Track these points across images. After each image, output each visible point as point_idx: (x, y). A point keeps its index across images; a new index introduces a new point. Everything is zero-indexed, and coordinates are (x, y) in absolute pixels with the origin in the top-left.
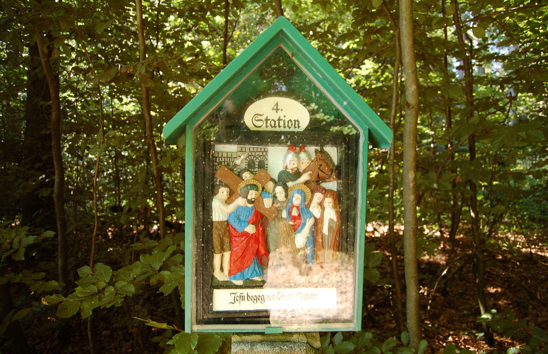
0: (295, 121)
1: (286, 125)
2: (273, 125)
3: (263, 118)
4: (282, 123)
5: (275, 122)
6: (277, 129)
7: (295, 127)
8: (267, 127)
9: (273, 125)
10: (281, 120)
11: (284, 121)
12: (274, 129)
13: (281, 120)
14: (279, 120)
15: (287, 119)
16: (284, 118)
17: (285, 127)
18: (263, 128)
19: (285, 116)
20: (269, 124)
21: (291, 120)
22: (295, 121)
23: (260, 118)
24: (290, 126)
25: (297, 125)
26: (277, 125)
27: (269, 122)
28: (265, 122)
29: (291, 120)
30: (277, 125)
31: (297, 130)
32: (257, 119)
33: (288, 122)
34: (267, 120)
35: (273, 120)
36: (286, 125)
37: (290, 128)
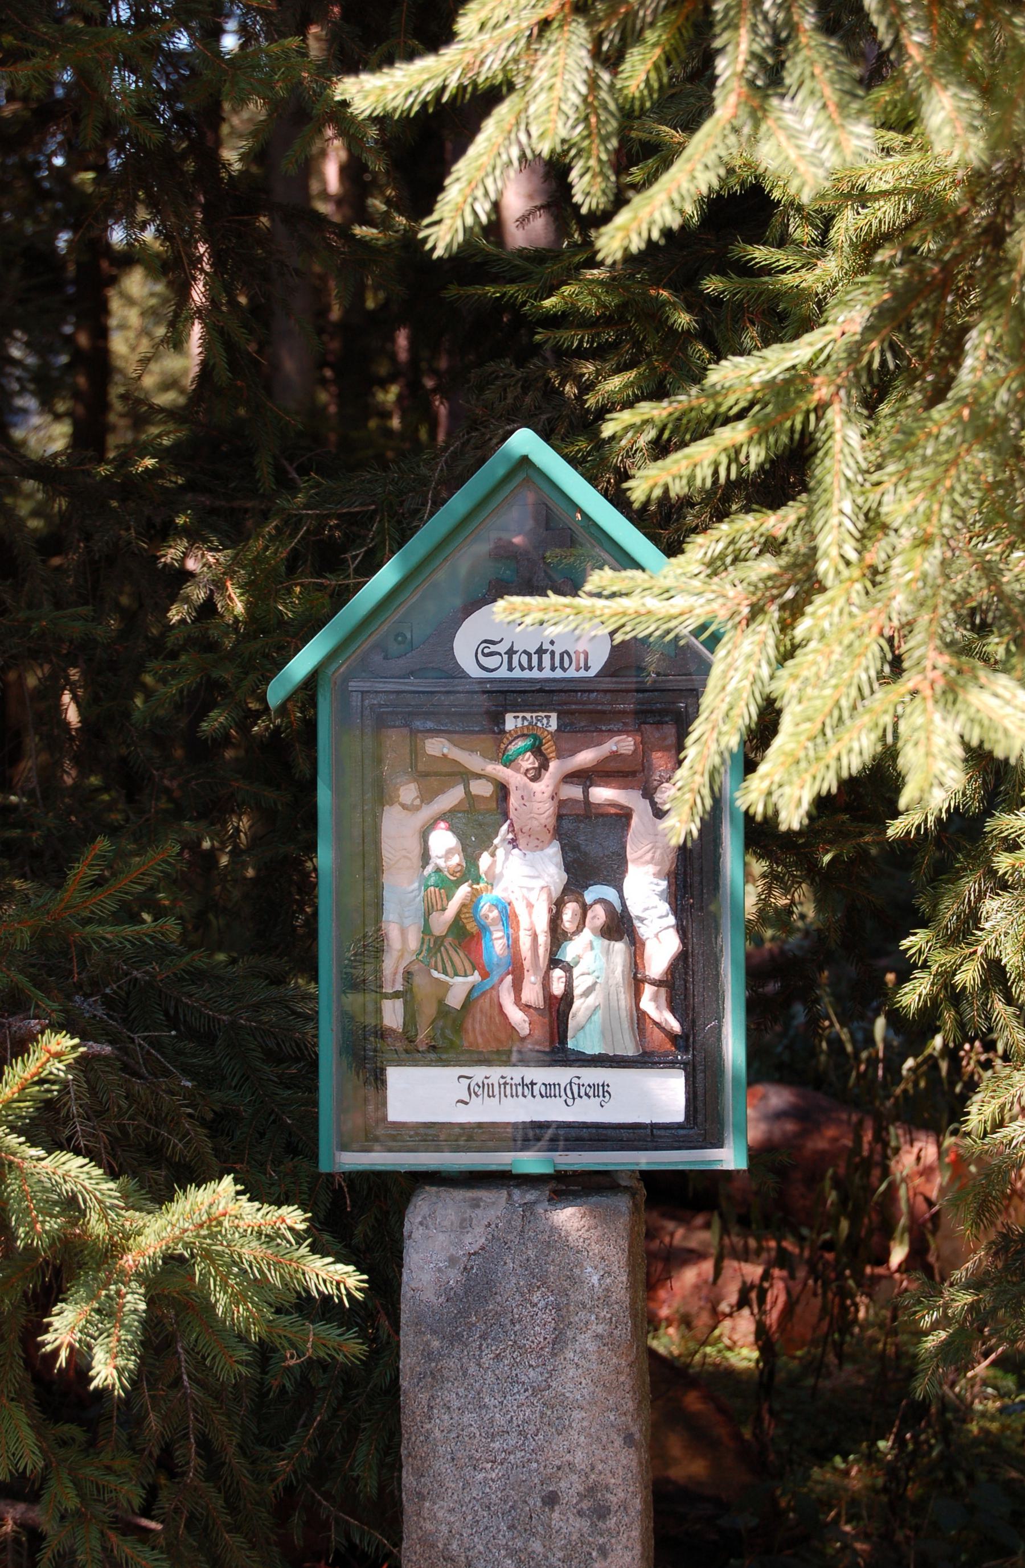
2: (525, 665)
3: (502, 648)
4: (546, 658)
5: (529, 655)
6: (535, 674)
8: (510, 669)
9: (525, 665)
11: (553, 653)
12: (527, 674)
14: (540, 651)
15: (558, 649)
16: (551, 648)
17: (553, 668)
18: (503, 673)
19: (552, 643)
20: (515, 663)
23: (493, 648)
25: (582, 664)
27: (515, 657)
28: (506, 657)
29: (567, 652)
31: (582, 673)
32: (486, 651)
34: (511, 652)
35: (525, 652)
36: (557, 663)
37: (564, 670)
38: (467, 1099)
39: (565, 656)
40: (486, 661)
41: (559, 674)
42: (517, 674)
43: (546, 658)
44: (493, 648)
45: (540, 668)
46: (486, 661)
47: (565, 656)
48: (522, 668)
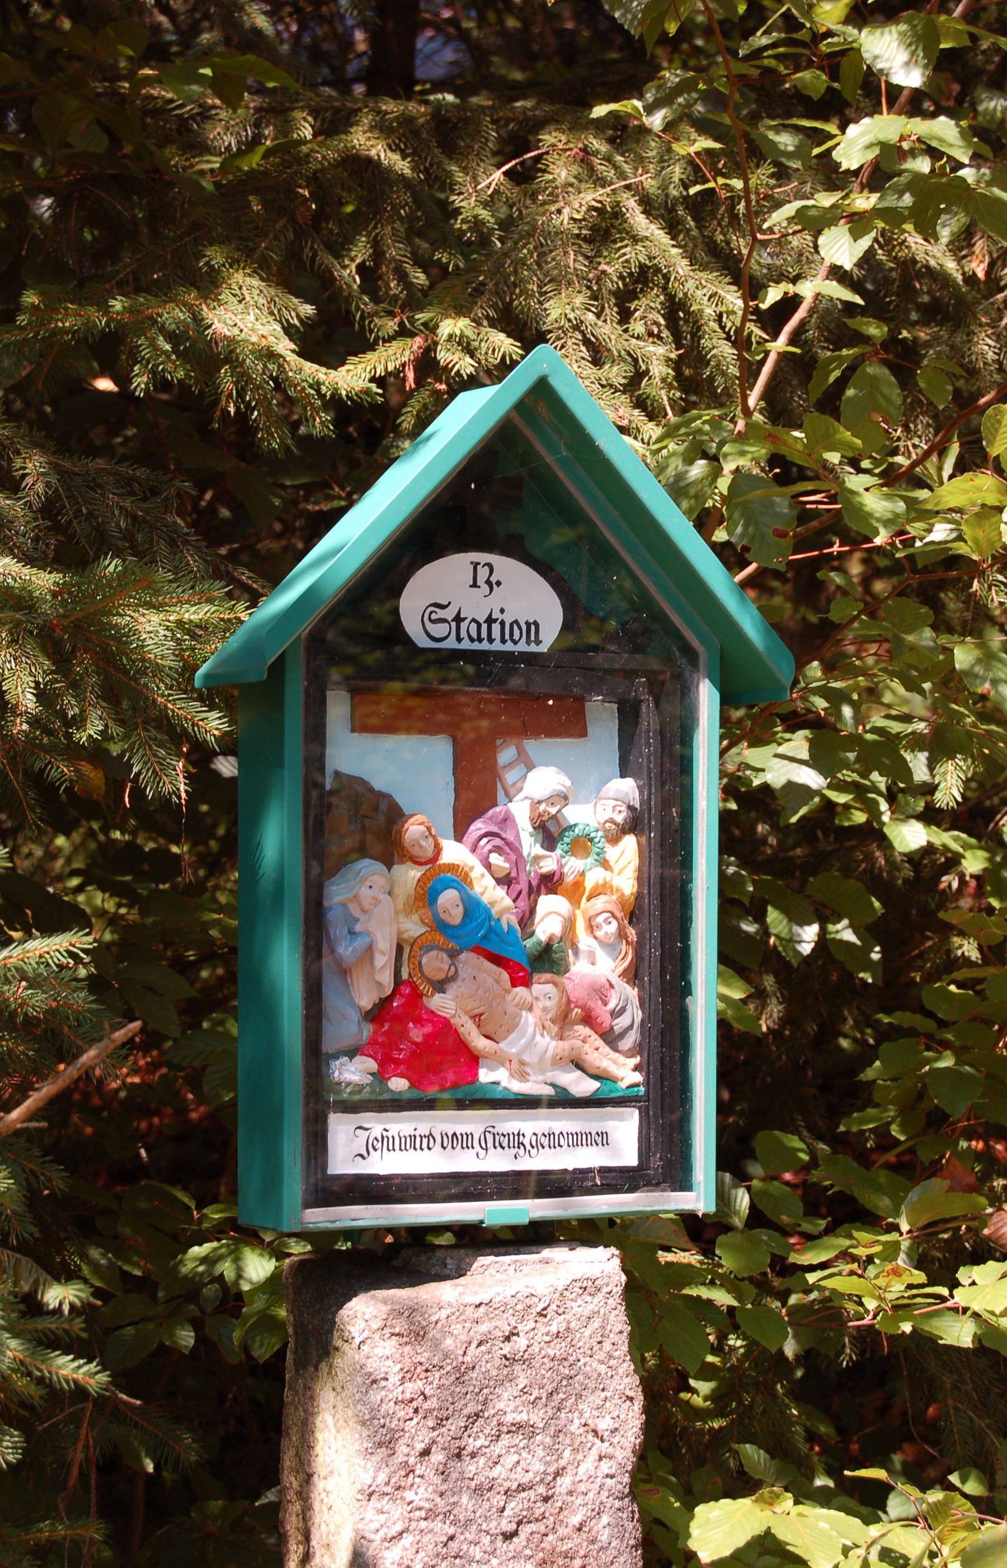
0: (528, 625)
1: (507, 637)
2: (475, 636)
3: (449, 614)
4: (496, 628)
5: (479, 626)
6: (485, 646)
7: (528, 642)
8: (459, 639)
9: (475, 636)
10: (495, 621)
11: (503, 623)
12: (476, 646)
13: (495, 621)
14: (490, 621)
16: (500, 617)
17: (503, 641)
18: (451, 643)
19: (502, 611)
20: (463, 634)
21: (516, 622)
22: (528, 625)
23: (441, 614)
24: (516, 637)
25: (533, 638)
26: (484, 634)
27: (464, 626)
28: (454, 624)
29: (516, 622)
30: (484, 634)
31: (533, 648)
32: (434, 617)
33: (511, 625)
34: (458, 619)
35: (474, 620)
36: (507, 637)
37: (515, 643)
38: (365, 1154)
39: (515, 626)
40: (432, 628)
41: (509, 647)
42: (466, 645)
43: (496, 628)
44: (441, 614)
45: (491, 640)
46: (432, 628)
47: (515, 626)
48: (472, 640)
